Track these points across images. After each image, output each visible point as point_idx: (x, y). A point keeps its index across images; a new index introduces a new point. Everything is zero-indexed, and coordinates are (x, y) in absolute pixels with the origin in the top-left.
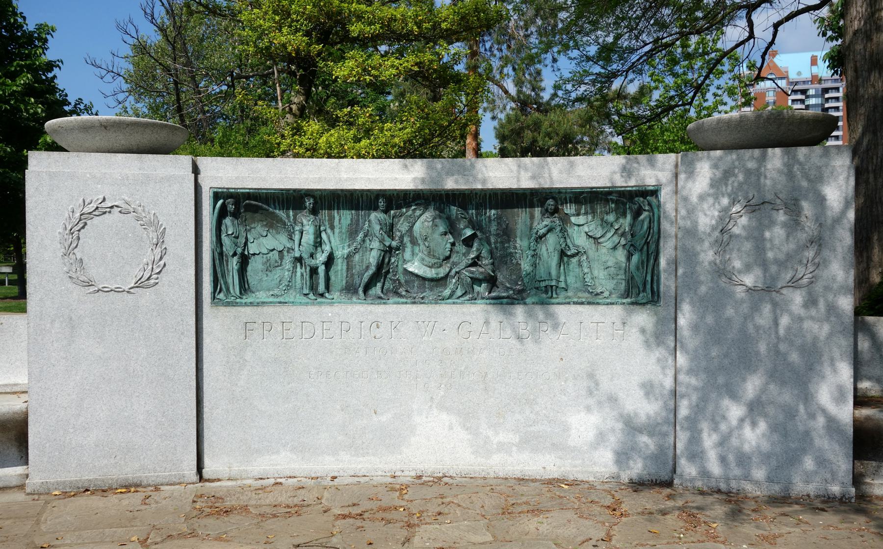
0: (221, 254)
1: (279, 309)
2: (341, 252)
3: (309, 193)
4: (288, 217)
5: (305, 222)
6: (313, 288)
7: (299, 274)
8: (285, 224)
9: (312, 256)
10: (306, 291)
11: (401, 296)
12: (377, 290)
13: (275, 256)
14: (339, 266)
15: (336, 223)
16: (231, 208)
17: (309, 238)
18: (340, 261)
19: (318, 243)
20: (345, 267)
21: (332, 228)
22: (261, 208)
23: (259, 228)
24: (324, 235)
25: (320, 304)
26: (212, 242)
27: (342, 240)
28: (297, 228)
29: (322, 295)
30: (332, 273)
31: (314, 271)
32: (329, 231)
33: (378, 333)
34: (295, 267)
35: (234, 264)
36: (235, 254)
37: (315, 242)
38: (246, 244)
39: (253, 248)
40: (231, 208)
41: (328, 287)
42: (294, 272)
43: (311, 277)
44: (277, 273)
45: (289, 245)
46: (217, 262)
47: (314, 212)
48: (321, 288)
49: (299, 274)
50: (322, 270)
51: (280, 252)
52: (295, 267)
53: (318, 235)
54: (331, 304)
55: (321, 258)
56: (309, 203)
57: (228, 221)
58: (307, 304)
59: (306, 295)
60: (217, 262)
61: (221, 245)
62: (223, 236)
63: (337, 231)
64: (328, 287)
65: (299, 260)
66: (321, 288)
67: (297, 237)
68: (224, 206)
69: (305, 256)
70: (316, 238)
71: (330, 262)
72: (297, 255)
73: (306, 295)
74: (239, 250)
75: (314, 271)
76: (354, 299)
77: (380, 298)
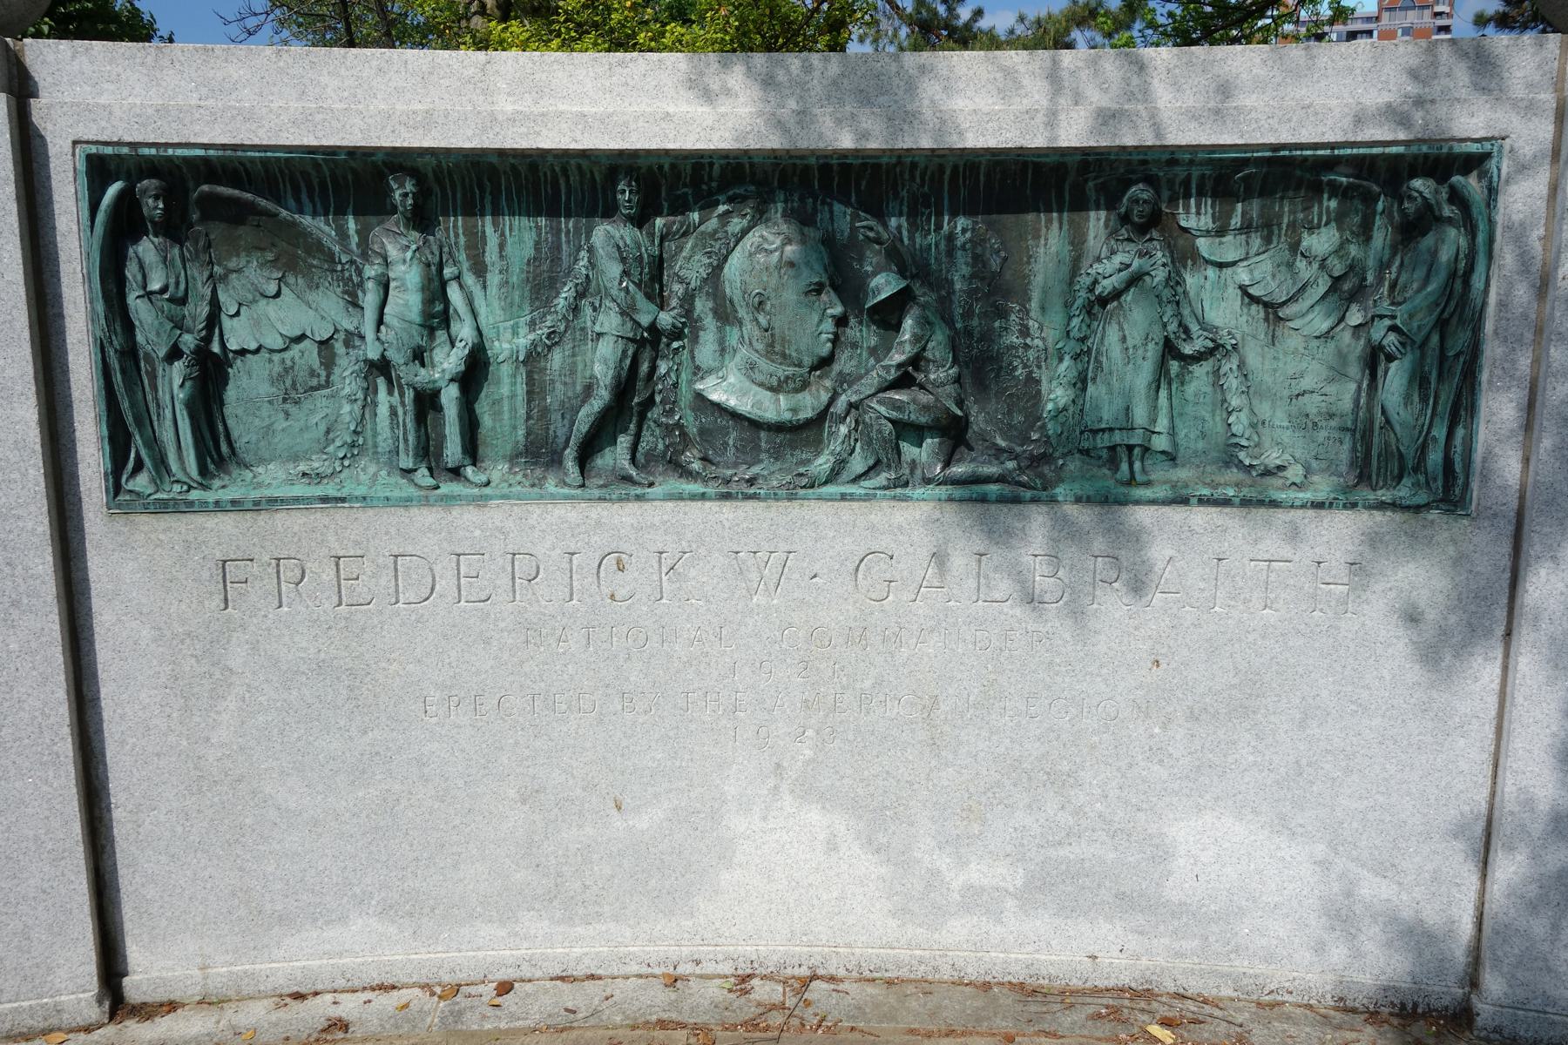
0: (130, 353)
1: (319, 518)
2: (508, 344)
3: (399, 161)
4: (343, 235)
5: (393, 252)
6: (428, 451)
7: (383, 411)
8: (331, 258)
9: (419, 356)
10: (407, 462)
11: (687, 474)
12: (616, 455)
13: (308, 355)
14: (505, 387)
15: (491, 254)
16: (153, 207)
17: (407, 301)
18: (506, 370)
19: (437, 317)
20: (521, 389)
21: (480, 270)
22: (251, 209)
23: (252, 273)
24: (454, 293)
25: (449, 500)
26: (93, 318)
27: (509, 307)
28: (371, 271)
29: (456, 473)
30: (483, 408)
31: (427, 402)
32: (469, 279)
33: (623, 584)
34: (369, 390)
35: (174, 382)
36: (174, 354)
37: (427, 315)
38: (213, 320)
39: (237, 334)
40: (153, 207)
41: (472, 449)
42: (369, 404)
43: (420, 419)
44: (318, 409)
45: (348, 324)
46: (118, 378)
47: (422, 219)
48: (453, 450)
49: (383, 411)
50: (450, 396)
51: (324, 344)
52: (369, 390)
53: (435, 291)
54: (480, 501)
55: (448, 361)
56: (402, 191)
57: (147, 249)
58: (406, 503)
59: (407, 472)
60: (118, 378)
61: (129, 327)
62: (133, 299)
63: (494, 279)
64: (472, 449)
65: (382, 367)
66: (453, 450)
67: (370, 299)
68: (127, 200)
69: (396, 357)
70: (428, 302)
71: (475, 372)
72: (373, 354)
73: (407, 472)
74: (189, 341)
75: (427, 402)
76: (551, 486)
77: (627, 479)
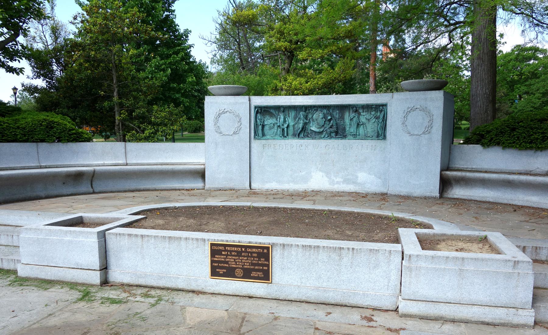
0: (257, 124)
1: (273, 141)
2: (292, 124)
3: (282, 106)
4: (276, 114)
5: (281, 115)
6: (283, 135)
7: (279, 131)
8: (275, 115)
9: (283, 125)
10: (281, 136)
11: (309, 137)
12: (302, 135)
13: (272, 125)
14: (291, 128)
15: (290, 115)
16: (260, 111)
17: (282, 120)
18: (291, 127)
19: (285, 121)
20: (292, 128)
21: (289, 117)
22: (268, 111)
23: (268, 117)
24: (286, 119)
25: (285, 139)
26: (254, 121)
27: (292, 120)
28: (279, 117)
29: (286, 137)
30: (289, 130)
31: (283, 130)
32: (288, 117)
33: (302, 148)
34: (278, 128)
35: (260, 127)
36: (261, 124)
37: (284, 121)
38: (264, 121)
39: (266, 123)
40: (260, 111)
41: (287, 135)
42: (278, 130)
43: (282, 131)
44: (273, 130)
45: (276, 122)
46: (256, 127)
47: (283, 111)
48: (286, 135)
49: (279, 131)
50: (285, 129)
51: (274, 124)
52: (278, 128)
53: (285, 119)
54: (288, 139)
55: (286, 126)
56: (282, 109)
57: (259, 115)
58: (281, 139)
59: (281, 137)
60: (256, 127)
61: (257, 122)
62: (257, 119)
63: (290, 117)
64: (287, 135)
65: (279, 126)
66: (286, 135)
67: (278, 120)
68: (257, 110)
69: (281, 125)
70: (284, 120)
71: (288, 127)
72: (278, 125)
73: (281, 137)
74: (262, 124)
75: (283, 130)
76: (295, 138)
77: (303, 138)
